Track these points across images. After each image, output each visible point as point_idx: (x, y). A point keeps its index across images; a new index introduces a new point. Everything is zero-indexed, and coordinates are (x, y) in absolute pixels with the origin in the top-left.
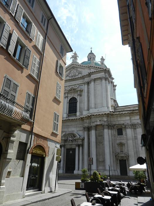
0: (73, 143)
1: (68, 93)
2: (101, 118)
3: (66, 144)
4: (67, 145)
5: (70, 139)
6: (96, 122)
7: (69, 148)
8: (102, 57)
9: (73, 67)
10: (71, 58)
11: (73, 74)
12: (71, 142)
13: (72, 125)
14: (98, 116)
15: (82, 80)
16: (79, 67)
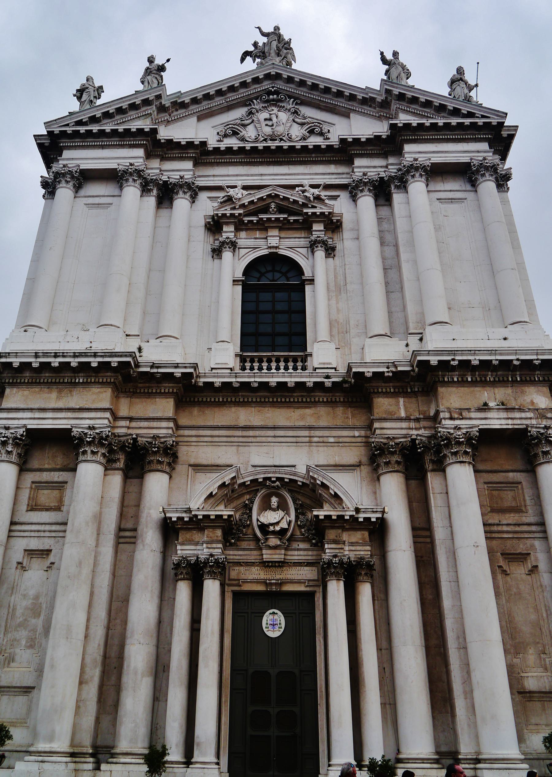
0: (295, 556)
1: (240, 226)
2: (509, 391)
3: (234, 555)
4: (239, 564)
5: (270, 517)
6: (480, 410)
7: (261, 588)
8: (460, 71)
9: (269, 93)
10: (246, 54)
11: (268, 130)
12: (273, 541)
13: (274, 428)
14: (490, 378)
15: (332, 168)
16: (315, 96)
